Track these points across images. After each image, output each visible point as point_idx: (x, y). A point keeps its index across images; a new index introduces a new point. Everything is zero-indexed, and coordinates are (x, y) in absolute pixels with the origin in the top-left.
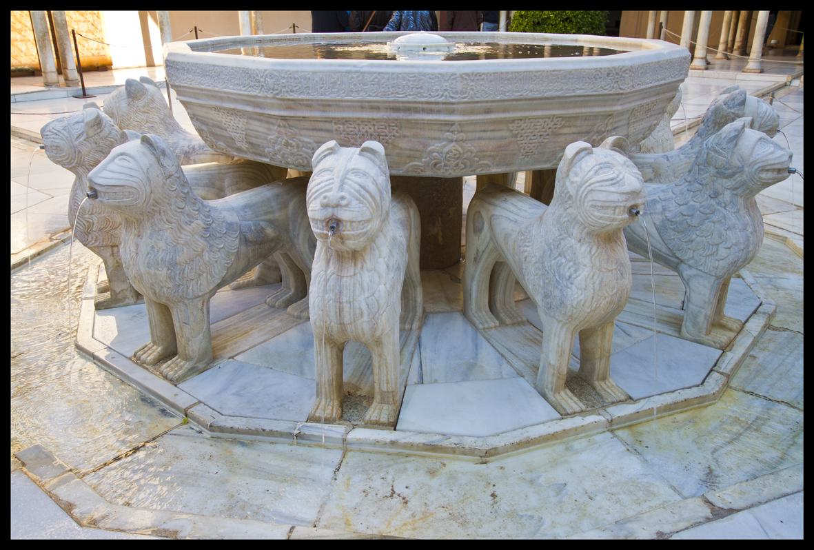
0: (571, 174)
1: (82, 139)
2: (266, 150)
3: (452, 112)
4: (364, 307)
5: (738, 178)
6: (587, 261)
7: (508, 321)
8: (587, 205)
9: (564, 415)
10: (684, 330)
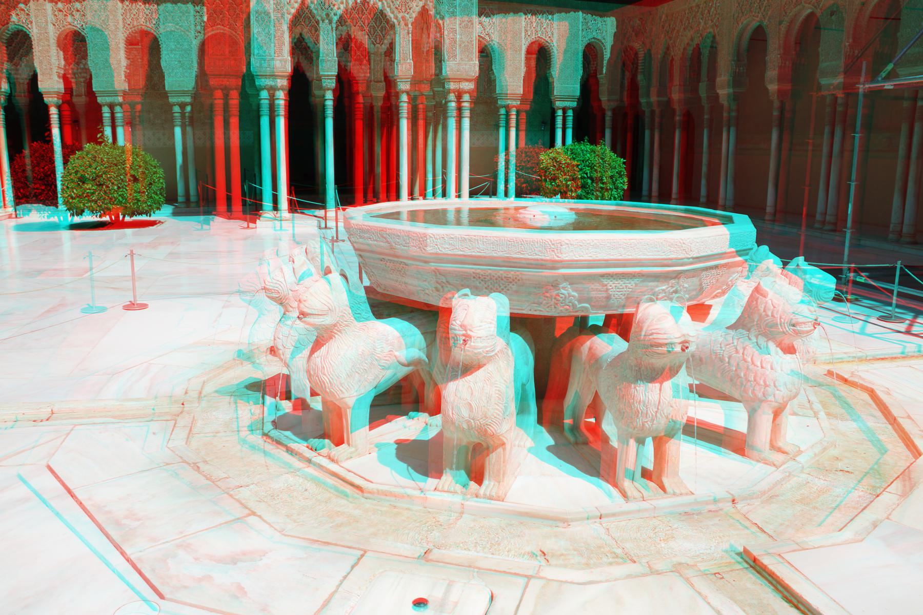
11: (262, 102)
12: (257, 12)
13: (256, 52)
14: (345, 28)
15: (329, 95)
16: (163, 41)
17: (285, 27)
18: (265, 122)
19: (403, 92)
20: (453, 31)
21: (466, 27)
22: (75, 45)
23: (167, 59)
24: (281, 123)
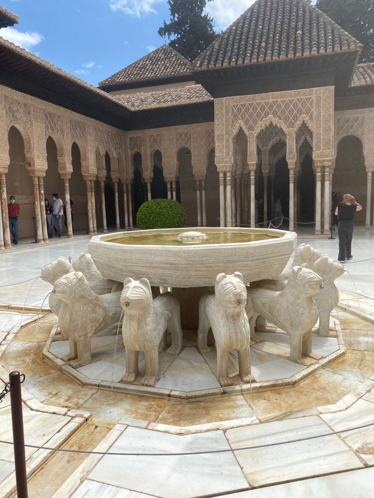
0: (298, 277)
1: (78, 284)
2: (169, 281)
3: (248, 261)
4: (245, 332)
5: (331, 275)
6: (307, 306)
7: (258, 341)
8: (307, 286)
9: (308, 366)
10: (321, 333)
11: (220, 179)
12: (218, 135)
13: (217, 155)
14: (278, 137)
15: (252, 174)
16: (192, 151)
17: (231, 141)
18: (221, 188)
19: (291, 169)
20: (319, 134)
21: (326, 131)
22: (157, 155)
23: (194, 160)
24: (229, 188)
